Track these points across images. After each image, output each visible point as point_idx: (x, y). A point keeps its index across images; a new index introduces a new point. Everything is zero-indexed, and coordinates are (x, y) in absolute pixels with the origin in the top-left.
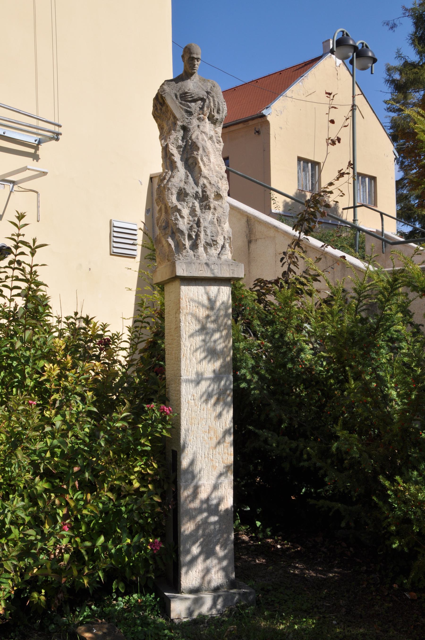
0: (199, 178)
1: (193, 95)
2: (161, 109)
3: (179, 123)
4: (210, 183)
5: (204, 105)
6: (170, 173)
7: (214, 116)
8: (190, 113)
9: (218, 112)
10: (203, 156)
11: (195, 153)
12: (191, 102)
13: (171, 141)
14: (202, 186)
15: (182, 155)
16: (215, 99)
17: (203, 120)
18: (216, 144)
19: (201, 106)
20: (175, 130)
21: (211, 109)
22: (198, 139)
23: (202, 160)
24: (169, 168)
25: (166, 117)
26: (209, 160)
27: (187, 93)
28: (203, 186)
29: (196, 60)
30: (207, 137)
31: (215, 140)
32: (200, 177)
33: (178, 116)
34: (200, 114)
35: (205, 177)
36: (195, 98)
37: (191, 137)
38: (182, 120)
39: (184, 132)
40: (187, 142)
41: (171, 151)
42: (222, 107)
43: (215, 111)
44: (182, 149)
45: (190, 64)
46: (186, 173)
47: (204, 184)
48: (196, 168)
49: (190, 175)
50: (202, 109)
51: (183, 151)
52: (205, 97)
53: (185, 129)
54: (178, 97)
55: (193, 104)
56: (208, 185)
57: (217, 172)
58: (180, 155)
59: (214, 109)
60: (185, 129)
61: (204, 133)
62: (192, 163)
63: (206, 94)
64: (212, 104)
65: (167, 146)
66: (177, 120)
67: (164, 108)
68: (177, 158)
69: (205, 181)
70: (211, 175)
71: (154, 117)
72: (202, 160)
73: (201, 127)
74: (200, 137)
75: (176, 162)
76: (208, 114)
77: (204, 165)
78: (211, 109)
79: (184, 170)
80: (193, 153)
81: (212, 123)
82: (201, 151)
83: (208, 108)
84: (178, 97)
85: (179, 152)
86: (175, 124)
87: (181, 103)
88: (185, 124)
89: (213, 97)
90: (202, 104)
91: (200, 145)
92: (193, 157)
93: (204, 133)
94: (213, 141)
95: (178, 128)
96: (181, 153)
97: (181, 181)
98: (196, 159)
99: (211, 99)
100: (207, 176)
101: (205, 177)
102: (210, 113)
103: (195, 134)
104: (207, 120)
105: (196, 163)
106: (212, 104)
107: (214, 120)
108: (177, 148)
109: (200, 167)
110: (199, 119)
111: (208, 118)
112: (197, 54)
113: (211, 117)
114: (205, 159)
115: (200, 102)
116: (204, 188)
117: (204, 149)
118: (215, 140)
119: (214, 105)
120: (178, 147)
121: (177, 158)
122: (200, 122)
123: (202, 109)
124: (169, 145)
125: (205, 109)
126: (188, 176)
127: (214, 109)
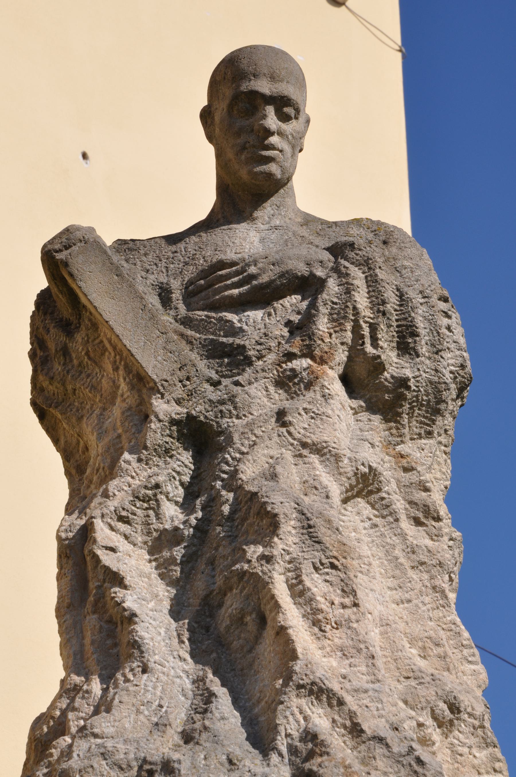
0: (276, 701)
1: (253, 270)
2: (65, 352)
3: (163, 407)
4: (355, 730)
5: (313, 305)
6: (96, 687)
7: (377, 366)
8: (232, 357)
9: (405, 347)
10: (307, 568)
11: (254, 551)
12: (241, 305)
13: (112, 504)
14: (293, 750)
15: (182, 585)
16: (381, 275)
17: (309, 386)
18: (405, 525)
19: (296, 318)
20: (138, 447)
21: (356, 329)
22: (274, 476)
23: (299, 591)
24: (92, 663)
25: (94, 388)
26: (349, 591)
27: (222, 265)
28: (303, 748)
29: (270, 110)
30: (338, 472)
31: (399, 505)
32: (280, 692)
33: (153, 364)
34: (290, 356)
35: (318, 691)
36: (264, 279)
37: (234, 474)
38: (179, 392)
39: (197, 458)
40: (212, 504)
41: (107, 559)
42: (435, 330)
43: (386, 337)
44: (178, 552)
45: (238, 134)
46: (199, 681)
47: (310, 736)
48: (267, 648)
49: (222, 694)
50: (301, 328)
51: (189, 560)
52: (320, 273)
53: (201, 438)
54: (177, 295)
55: (256, 315)
56: (338, 742)
57: (412, 675)
58: (171, 583)
59: (373, 328)
60: (201, 438)
61: (318, 449)
62: (239, 620)
63: (327, 256)
64: (362, 300)
65: (86, 532)
66: (154, 390)
67: (78, 344)
68: (147, 596)
69: (321, 719)
70: (362, 681)
71: (42, 415)
72: (299, 591)
73: (300, 424)
74: (292, 474)
75: (131, 618)
76: (341, 356)
77: (316, 620)
78: (356, 329)
79: (190, 665)
80: (243, 557)
81: (372, 408)
82: (288, 539)
83: (337, 320)
84: (177, 295)
85: (163, 568)
86: (143, 416)
87: (186, 322)
88: (199, 409)
89: (366, 264)
90: (305, 304)
91: (280, 503)
92: (243, 574)
93: (318, 449)
94: (385, 509)
95: (156, 433)
96: (177, 571)
97: (160, 726)
98: (257, 588)
99: (358, 277)
100: (335, 686)
101: (318, 691)
102: (355, 350)
103: (259, 460)
104: (337, 388)
105: (262, 612)
106: (362, 300)
107: (381, 388)
108: (154, 550)
109: (282, 631)
110: (287, 382)
111: (345, 379)
112: (273, 78)
113: (361, 370)
114: (316, 584)
115: (295, 299)
116: (311, 755)
117: (308, 529)
118: (399, 505)
119: (378, 303)
120: (160, 542)
121: (147, 596)
122: (292, 395)
123: (301, 328)
124: (99, 524)
125: (322, 324)
126: (209, 697)
127: (373, 328)
